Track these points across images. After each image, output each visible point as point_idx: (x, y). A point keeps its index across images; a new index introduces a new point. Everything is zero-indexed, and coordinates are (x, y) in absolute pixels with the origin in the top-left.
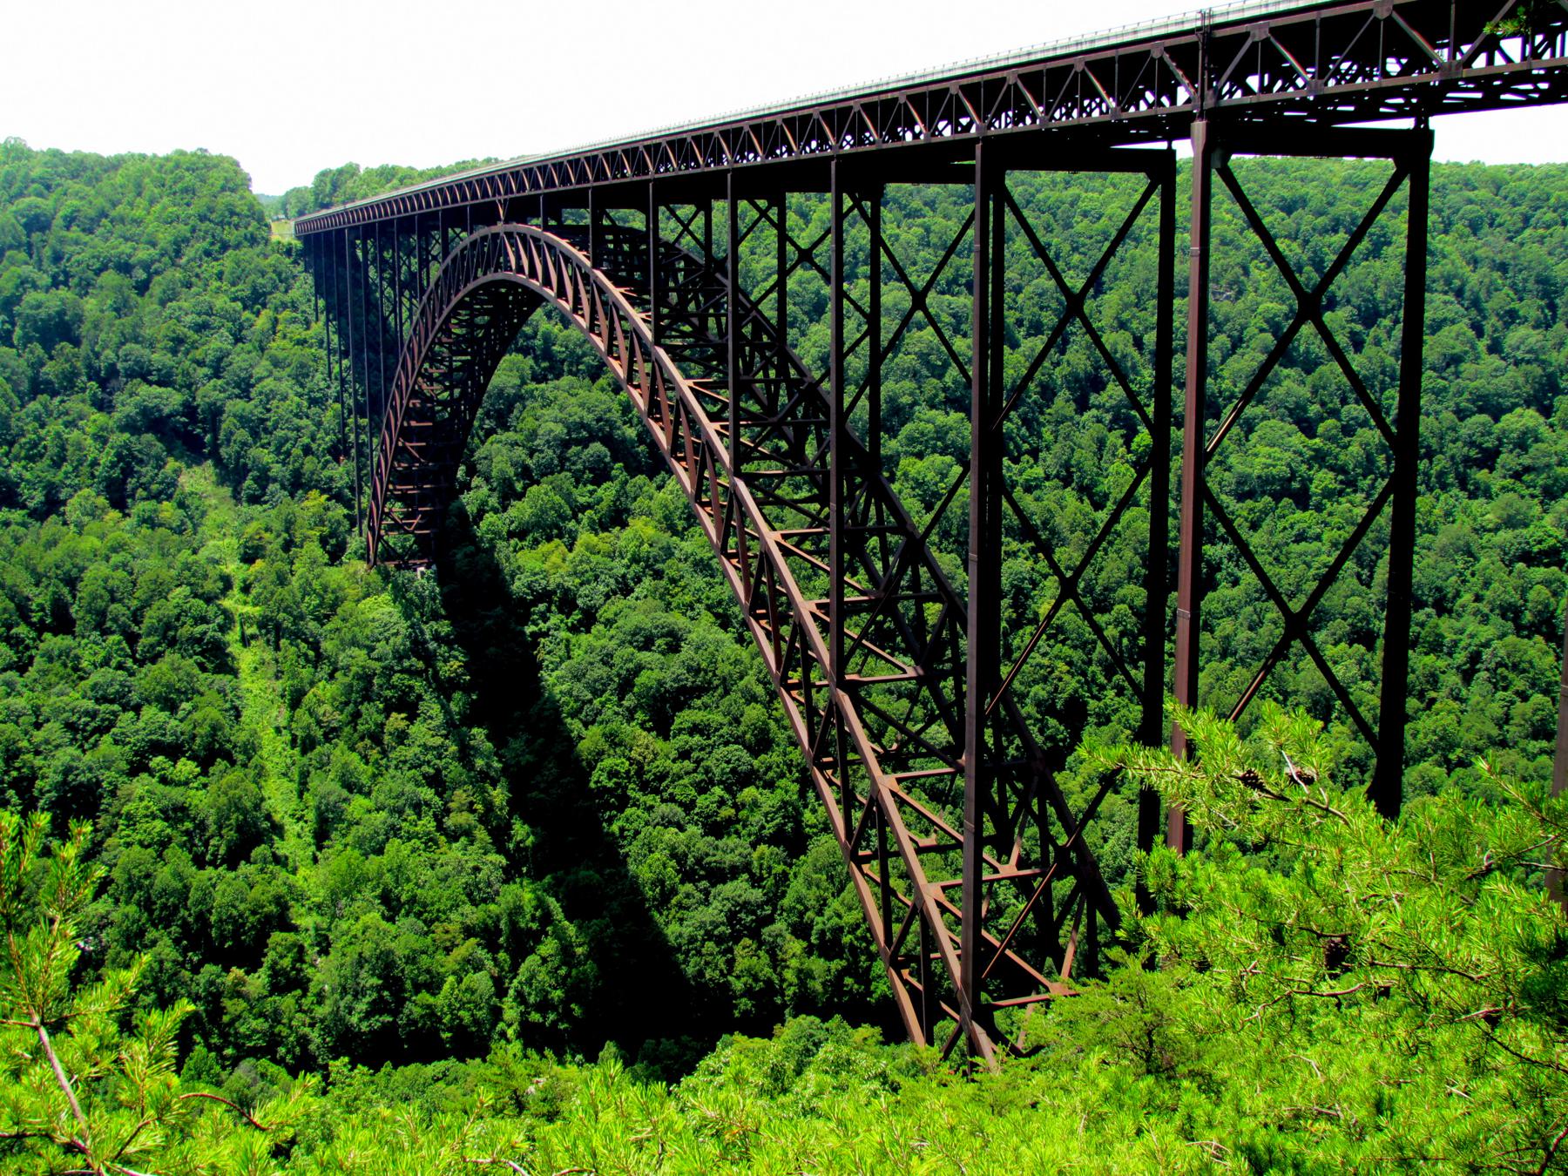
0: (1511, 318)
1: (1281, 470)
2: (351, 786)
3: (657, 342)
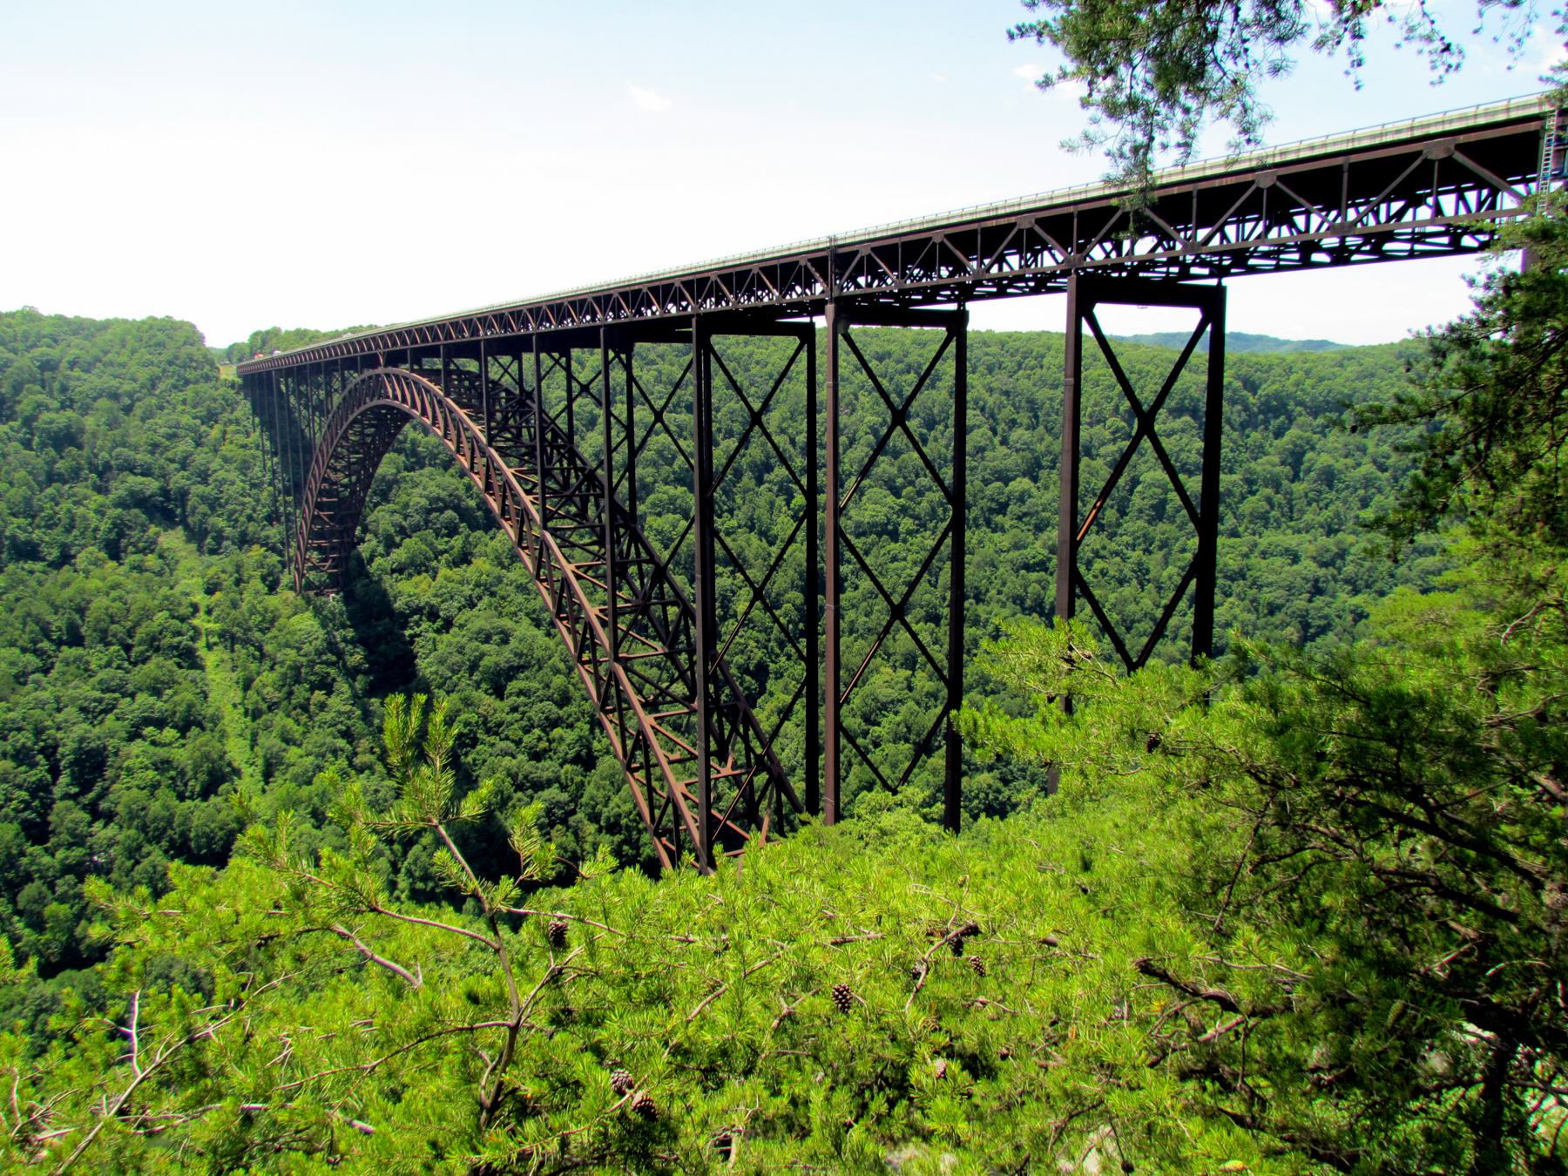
0: (1013, 424)
1: (881, 518)
2: (288, 740)
3: (490, 444)
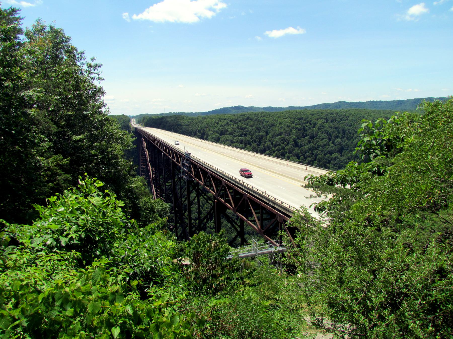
0: (337, 137)
